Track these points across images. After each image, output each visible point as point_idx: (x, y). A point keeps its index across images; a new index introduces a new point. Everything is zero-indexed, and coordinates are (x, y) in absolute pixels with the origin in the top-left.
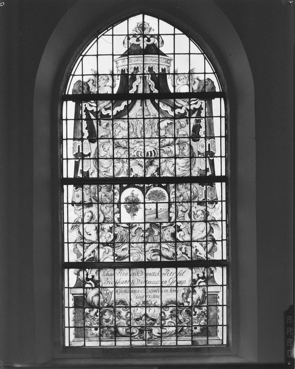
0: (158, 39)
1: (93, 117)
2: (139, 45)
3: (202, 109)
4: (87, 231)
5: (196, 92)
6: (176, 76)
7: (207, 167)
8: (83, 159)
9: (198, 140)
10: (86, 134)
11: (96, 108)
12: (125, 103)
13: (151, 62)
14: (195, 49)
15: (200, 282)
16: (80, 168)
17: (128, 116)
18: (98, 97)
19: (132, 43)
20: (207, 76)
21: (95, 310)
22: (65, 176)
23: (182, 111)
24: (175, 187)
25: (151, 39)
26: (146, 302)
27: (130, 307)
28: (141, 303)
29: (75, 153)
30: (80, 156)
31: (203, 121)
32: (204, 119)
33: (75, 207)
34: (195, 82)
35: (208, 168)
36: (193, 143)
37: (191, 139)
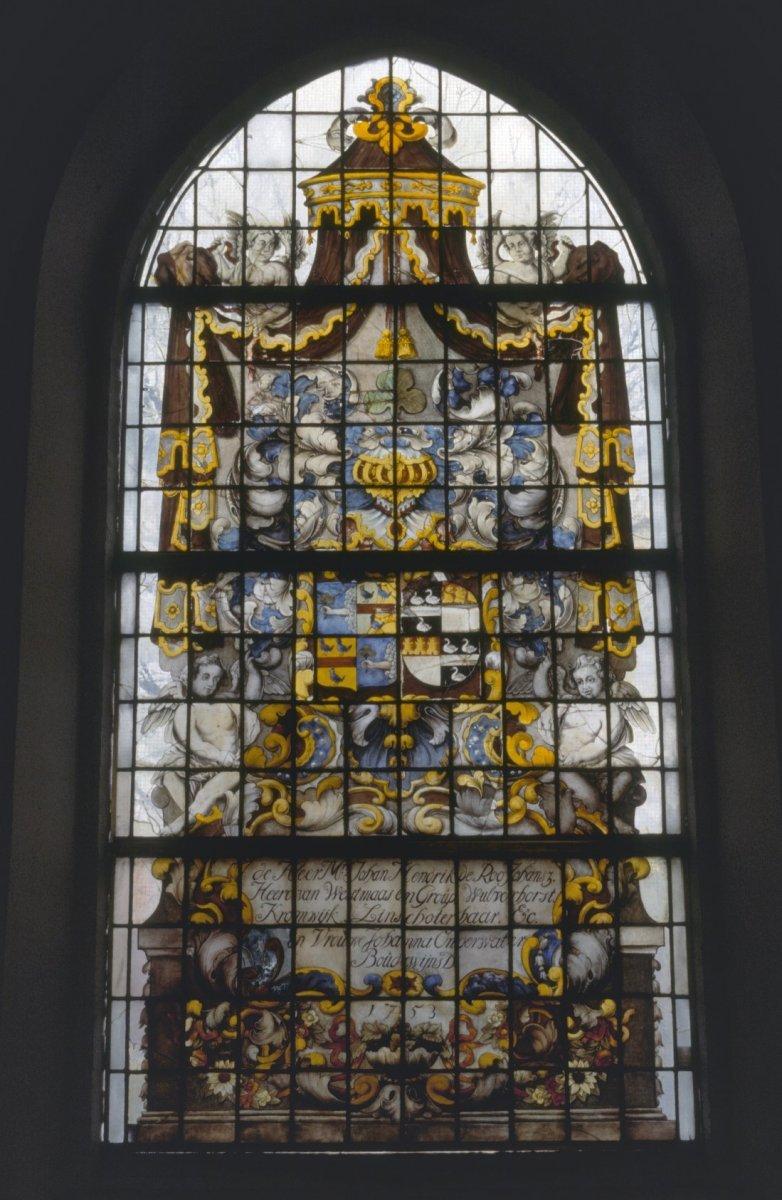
0: (437, 125)
1: (229, 356)
2: (377, 142)
3: (586, 335)
4: (204, 728)
5: (560, 282)
6: (496, 239)
7: (607, 520)
8: (191, 489)
9: (576, 430)
10: (204, 406)
11: (240, 328)
12: (334, 316)
13: (416, 193)
14: (554, 153)
15: (593, 911)
16: (180, 517)
17: (344, 355)
18: (247, 296)
19: (355, 137)
20: (595, 236)
21: (223, 1007)
22: (129, 544)
23: (522, 342)
24: (497, 583)
25: (414, 126)
26: (403, 983)
27: (349, 998)
28: (388, 983)
29: (164, 471)
30: (180, 478)
31: (589, 369)
32: (592, 365)
33: (161, 648)
34: (556, 253)
35: (610, 524)
36: (560, 443)
37: (553, 428)
